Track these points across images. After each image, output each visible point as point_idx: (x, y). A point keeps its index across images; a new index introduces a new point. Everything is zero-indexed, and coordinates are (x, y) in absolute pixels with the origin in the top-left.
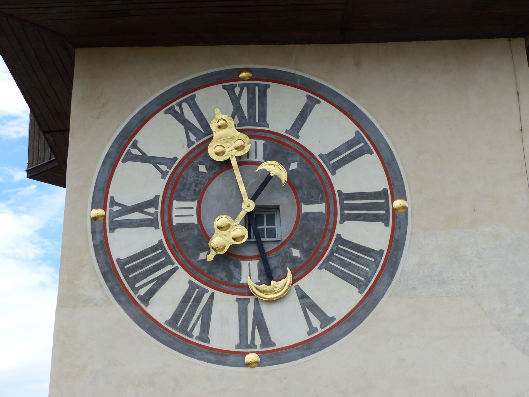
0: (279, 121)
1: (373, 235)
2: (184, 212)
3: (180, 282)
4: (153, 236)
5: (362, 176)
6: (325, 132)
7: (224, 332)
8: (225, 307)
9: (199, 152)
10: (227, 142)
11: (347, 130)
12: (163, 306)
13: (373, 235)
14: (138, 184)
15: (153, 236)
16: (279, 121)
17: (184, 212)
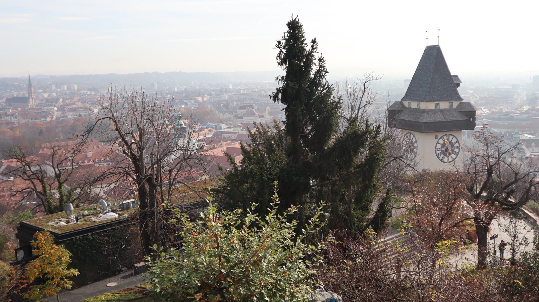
0: (450, 140)
1: (457, 150)
2: (443, 149)
3: (442, 155)
4: (440, 151)
5: (456, 145)
6: (454, 140)
7: (446, 161)
8: (446, 158)
9: (444, 143)
10: (447, 142)
11: (456, 140)
12: (441, 158)
13: (457, 150)
14: (439, 146)
15: (440, 151)
16: (450, 140)
17: (443, 149)
